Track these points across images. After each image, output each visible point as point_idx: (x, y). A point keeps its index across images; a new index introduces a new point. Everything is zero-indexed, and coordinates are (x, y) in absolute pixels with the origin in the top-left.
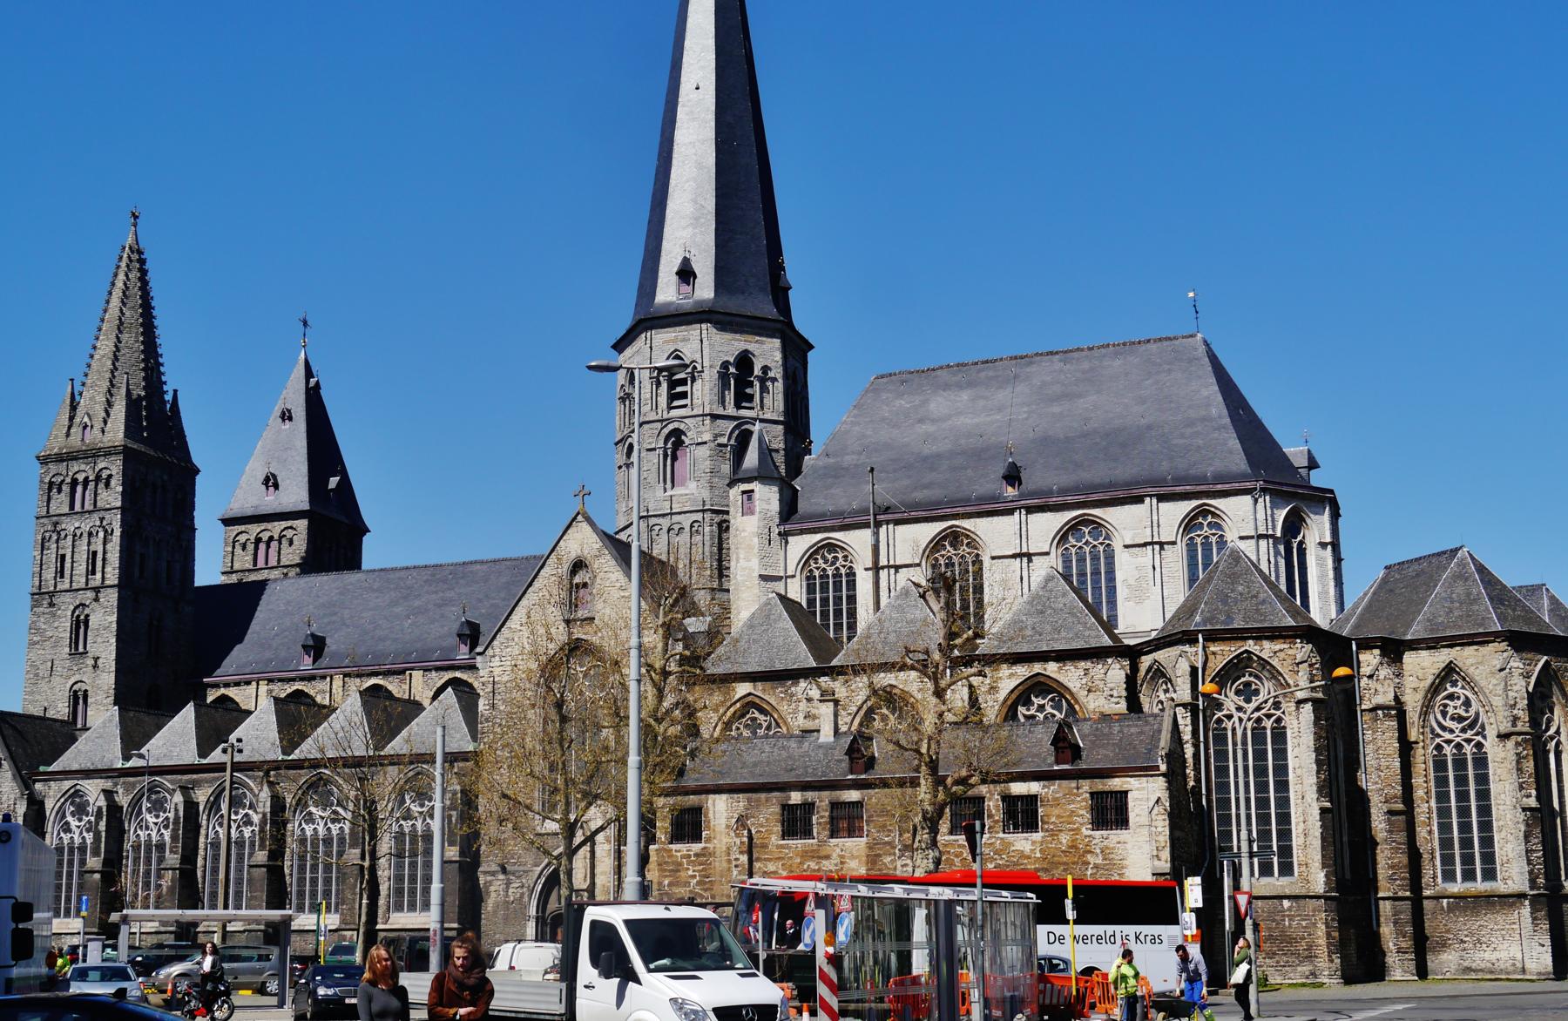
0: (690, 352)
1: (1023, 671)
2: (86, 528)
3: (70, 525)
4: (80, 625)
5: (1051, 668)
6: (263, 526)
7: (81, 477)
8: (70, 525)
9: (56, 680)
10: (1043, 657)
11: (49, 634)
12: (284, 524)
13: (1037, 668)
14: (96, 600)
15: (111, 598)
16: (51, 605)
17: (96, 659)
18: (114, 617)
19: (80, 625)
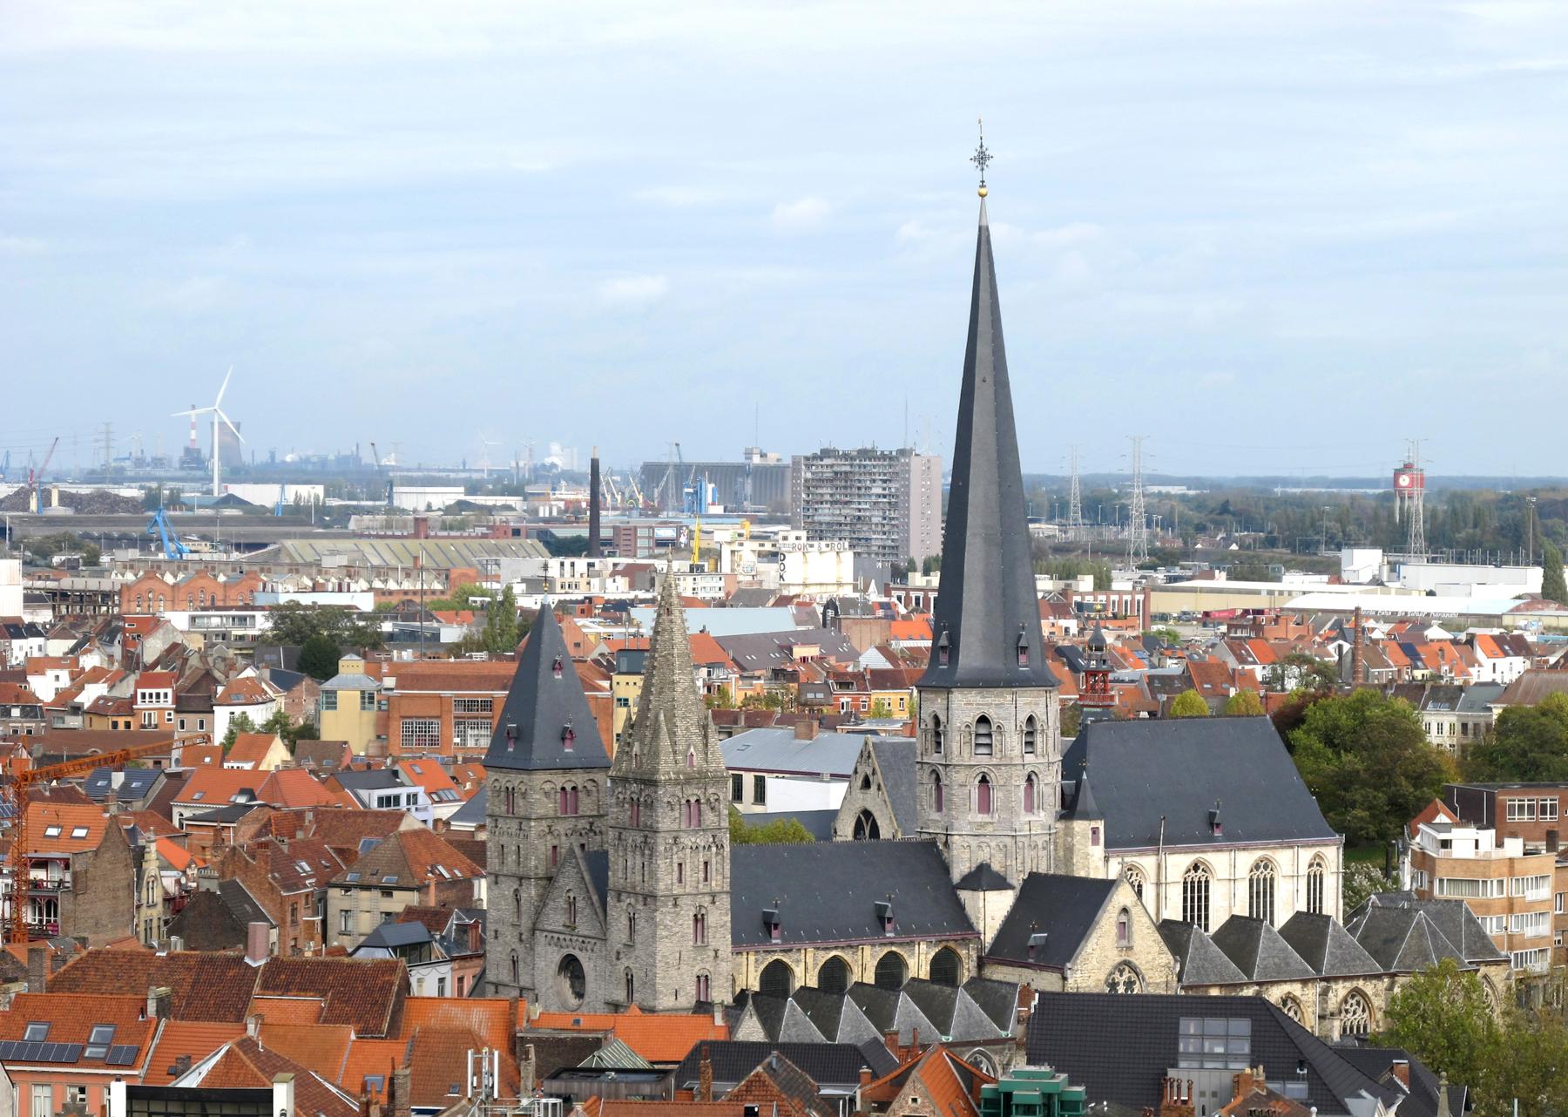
0: (1039, 713)
1: (1349, 985)
2: (701, 842)
3: (687, 840)
4: (699, 920)
5: (1360, 983)
6: (568, 776)
7: (693, 800)
8: (687, 840)
9: (684, 968)
10: (1358, 977)
11: (676, 929)
12: (587, 776)
13: (1355, 984)
14: (713, 902)
15: (725, 902)
16: (675, 905)
17: (716, 951)
18: (729, 918)
19: (699, 920)
